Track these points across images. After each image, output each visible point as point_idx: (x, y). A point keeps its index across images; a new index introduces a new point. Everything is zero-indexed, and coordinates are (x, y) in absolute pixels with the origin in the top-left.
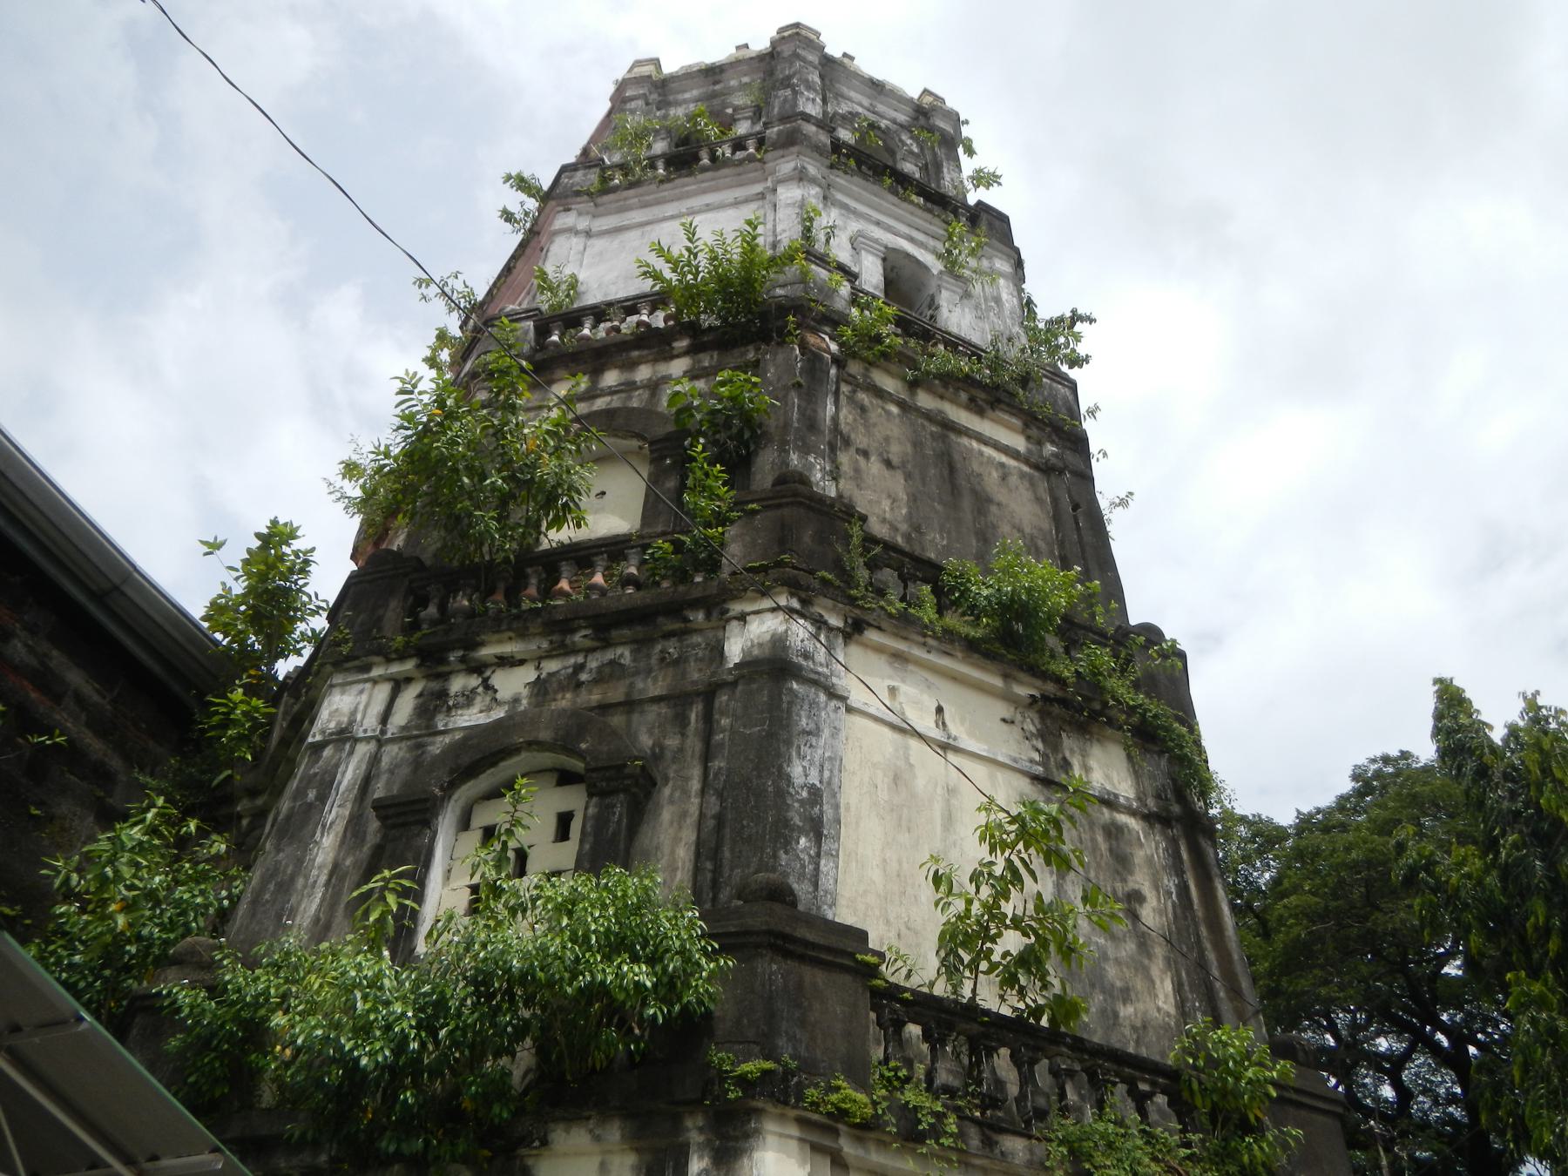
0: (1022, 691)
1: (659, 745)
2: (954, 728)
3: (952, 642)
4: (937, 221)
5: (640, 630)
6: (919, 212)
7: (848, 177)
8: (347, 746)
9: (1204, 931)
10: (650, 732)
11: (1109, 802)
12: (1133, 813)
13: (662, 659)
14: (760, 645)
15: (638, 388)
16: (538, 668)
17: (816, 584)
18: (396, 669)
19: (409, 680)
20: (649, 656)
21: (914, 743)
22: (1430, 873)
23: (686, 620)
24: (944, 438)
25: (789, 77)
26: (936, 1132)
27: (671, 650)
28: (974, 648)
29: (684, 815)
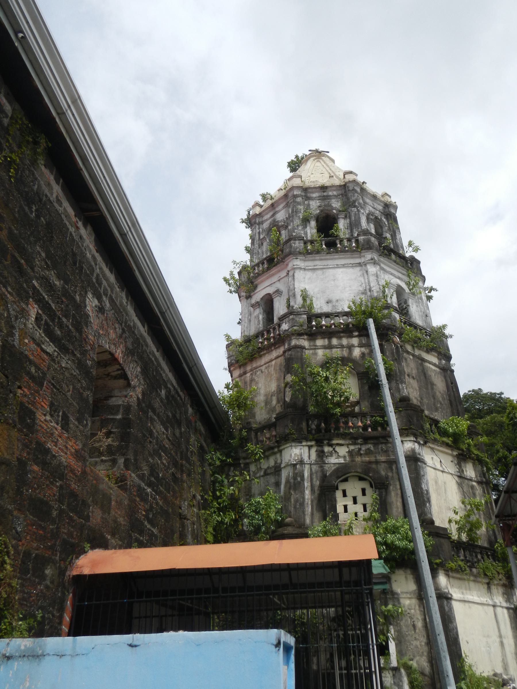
0: (455, 453)
1: (386, 474)
3: (443, 444)
4: (405, 270)
5: (375, 441)
6: (401, 267)
9: (491, 511)
10: (383, 470)
11: (471, 480)
12: (475, 481)
13: (382, 450)
15: (345, 347)
16: (348, 447)
17: (418, 434)
18: (309, 443)
19: (312, 446)
20: (378, 448)
21: (437, 472)
23: (387, 440)
24: (422, 364)
25: (354, 202)
26: (465, 570)
28: (447, 445)
29: (397, 494)
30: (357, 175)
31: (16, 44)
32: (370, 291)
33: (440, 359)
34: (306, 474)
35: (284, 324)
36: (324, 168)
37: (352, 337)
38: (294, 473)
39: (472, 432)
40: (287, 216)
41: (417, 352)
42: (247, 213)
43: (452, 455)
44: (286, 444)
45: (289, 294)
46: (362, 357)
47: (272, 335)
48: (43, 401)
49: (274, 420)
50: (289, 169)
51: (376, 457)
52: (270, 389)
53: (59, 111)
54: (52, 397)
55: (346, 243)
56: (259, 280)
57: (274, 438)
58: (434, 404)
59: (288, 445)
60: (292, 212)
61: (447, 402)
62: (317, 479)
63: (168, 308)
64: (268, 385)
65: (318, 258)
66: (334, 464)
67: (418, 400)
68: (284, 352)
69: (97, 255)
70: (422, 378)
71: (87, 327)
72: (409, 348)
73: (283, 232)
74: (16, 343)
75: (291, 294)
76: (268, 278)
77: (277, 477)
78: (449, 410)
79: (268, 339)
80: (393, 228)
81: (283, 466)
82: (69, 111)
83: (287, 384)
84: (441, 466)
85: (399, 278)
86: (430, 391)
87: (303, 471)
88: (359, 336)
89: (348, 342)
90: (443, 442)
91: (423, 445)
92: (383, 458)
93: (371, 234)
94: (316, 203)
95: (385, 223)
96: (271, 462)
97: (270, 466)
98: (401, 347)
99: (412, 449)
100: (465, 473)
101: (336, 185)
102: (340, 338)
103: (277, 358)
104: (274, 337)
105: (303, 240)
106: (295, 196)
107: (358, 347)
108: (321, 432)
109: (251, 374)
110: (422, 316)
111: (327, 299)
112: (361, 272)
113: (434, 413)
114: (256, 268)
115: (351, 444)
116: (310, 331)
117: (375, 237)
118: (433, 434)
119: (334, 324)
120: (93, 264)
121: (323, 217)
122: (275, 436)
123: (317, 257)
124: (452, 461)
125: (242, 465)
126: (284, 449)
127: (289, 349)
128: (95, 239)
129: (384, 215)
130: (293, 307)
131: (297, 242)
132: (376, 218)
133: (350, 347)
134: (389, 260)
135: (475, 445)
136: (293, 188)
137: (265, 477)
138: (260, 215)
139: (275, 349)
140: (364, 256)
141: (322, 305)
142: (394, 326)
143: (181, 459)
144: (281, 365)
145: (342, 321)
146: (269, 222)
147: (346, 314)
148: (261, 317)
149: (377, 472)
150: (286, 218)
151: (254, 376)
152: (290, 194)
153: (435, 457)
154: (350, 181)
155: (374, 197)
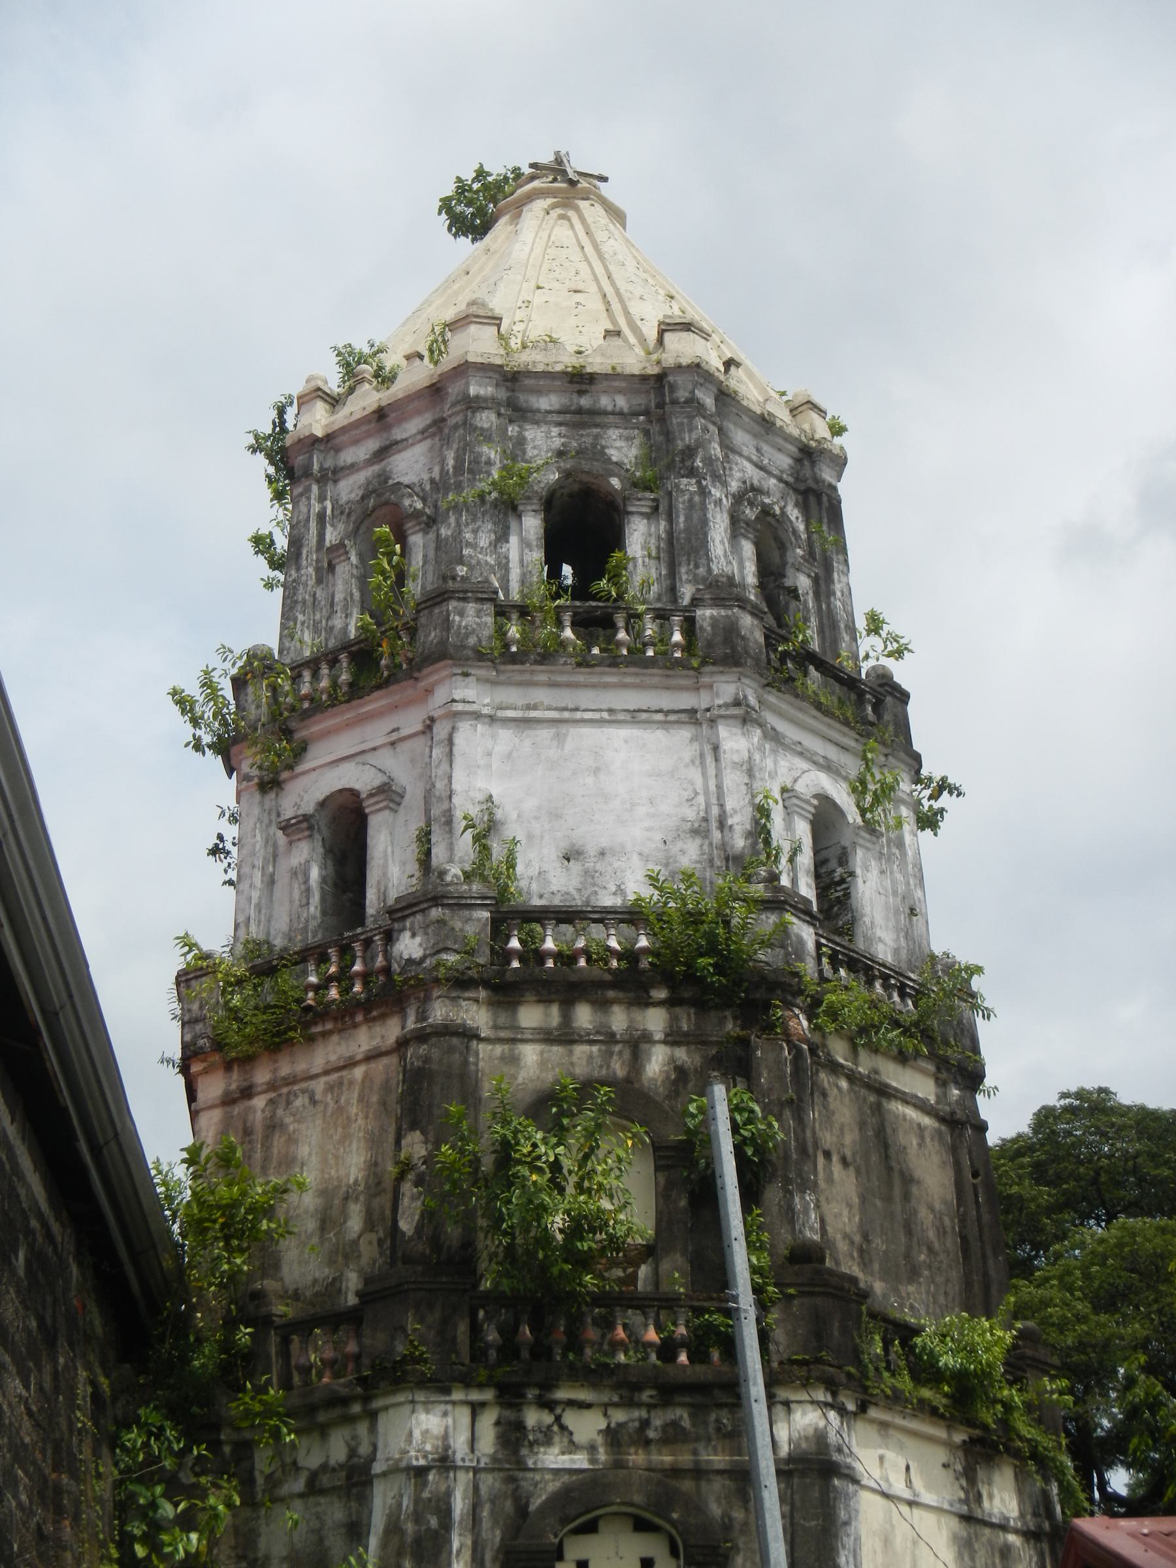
0: (959, 1437)
1: (726, 1515)
2: (918, 1483)
3: (922, 1410)
4: (853, 734)
6: (838, 725)
7: (780, 694)
8: (452, 1475)
10: (718, 1500)
11: (1003, 1527)
12: (1016, 1531)
13: (718, 1430)
14: (807, 1438)
15: (617, 1042)
16: (605, 1415)
17: (843, 1378)
18: (475, 1396)
19: (483, 1404)
20: (706, 1423)
22: (1153, 1414)
25: (690, 452)
27: (725, 1421)
30: (705, 335)
32: (722, 825)
33: (942, 1084)
34: (459, 1505)
35: (407, 934)
36: (587, 260)
37: (644, 1002)
38: (417, 1500)
39: (1022, 1357)
40: (436, 474)
41: (865, 1064)
42: (274, 414)
43: (948, 1445)
44: (394, 1392)
45: (427, 812)
46: (675, 1082)
47: (357, 967)
49: (352, 1300)
50: (444, 216)
51: (695, 1452)
52: (342, 1172)
55: (650, 629)
56: (316, 726)
57: (351, 1366)
58: (907, 1256)
59: (400, 1398)
60: (459, 468)
61: (952, 1243)
62: (495, 1522)
63: (71, 996)
64: (337, 1157)
65: (543, 678)
66: (557, 1472)
67: (852, 1243)
68: (402, 1044)
70: (874, 1158)
72: (839, 1051)
73: (417, 540)
75: (436, 812)
76: (349, 725)
77: (354, 1504)
78: (955, 1288)
79: (344, 978)
80: (824, 551)
81: (378, 1468)
83: (405, 1168)
84: (909, 1483)
85: (828, 767)
86: (898, 1208)
87: (449, 1494)
88: (670, 1003)
89: (631, 1021)
90: (921, 1401)
91: (855, 1414)
92: (718, 1459)
93: (743, 603)
94: (548, 436)
95: (795, 532)
96: (337, 1449)
97: (332, 1462)
98: (813, 1051)
99: (816, 1430)
100: (986, 1504)
101: (628, 371)
102: (603, 1005)
103: (372, 1056)
104: (366, 977)
105: (493, 600)
106: (473, 405)
107: (665, 1042)
108: (516, 1354)
109: (271, 1102)
110: (897, 912)
111: (564, 845)
112: (696, 745)
113: (902, 1288)
114: (307, 675)
115: (616, 1405)
116: (501, 973)
117: (753, 614)
118: (893, 1375)
119: (586, 952)
121: (571, 495)
122: (357, 1358)
123: (542, 674)
124: (945, 1466)
125: (227, 1449)
126: (386, 1408)
127: (421, 1037)
129: (796, 490)
130: (442, 874)
131: (471, 608)
132: (766, 511)
133: (637, 1044)
134: (798, 702)
135: (1029, 1407)
136: (464, 369)
137: (311, 1500)
138: (328, 442)
139: (368, 1020)
140: (710, 687)
141: (545, 867)
142: (796, 974)
143: (56, 1468)
144: (386, 1087)
145: (613, 943)
146: (361, 477)
147: (633, 916)
148: (315, 873)
149: (695, 1506)
150: (432, 481)
151: (280, 1112)
152: (454, 390)
153: (890, 1455)
154: (679, 367)
155: (766, 424)
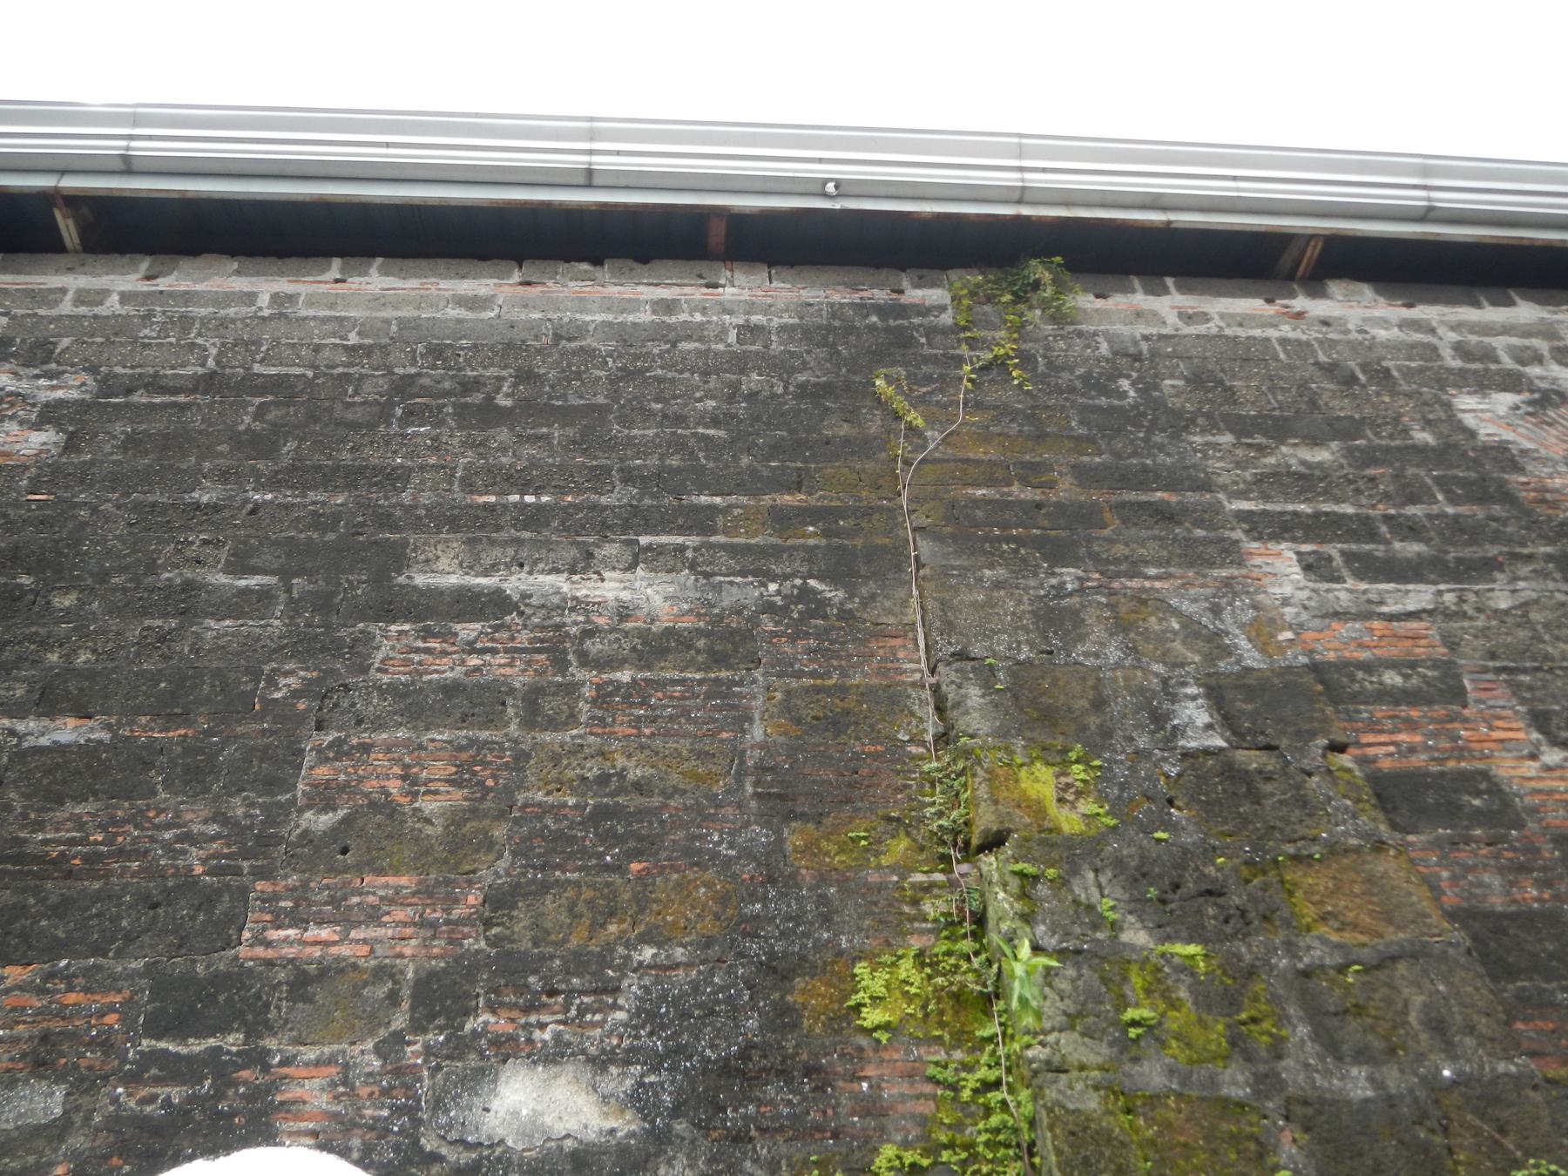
31: (838, 207)
48: (1491, 728)
53: (1016, 196)
54: (1523, 701)
69: (1424, 312)
71: (1520, 469)
74: (1252, 658)
82: (1028, 176)
120: (1418, 337)
128: (1378, 292)
